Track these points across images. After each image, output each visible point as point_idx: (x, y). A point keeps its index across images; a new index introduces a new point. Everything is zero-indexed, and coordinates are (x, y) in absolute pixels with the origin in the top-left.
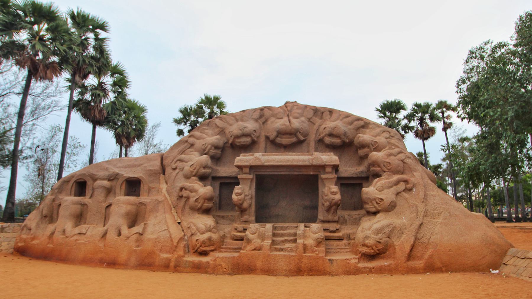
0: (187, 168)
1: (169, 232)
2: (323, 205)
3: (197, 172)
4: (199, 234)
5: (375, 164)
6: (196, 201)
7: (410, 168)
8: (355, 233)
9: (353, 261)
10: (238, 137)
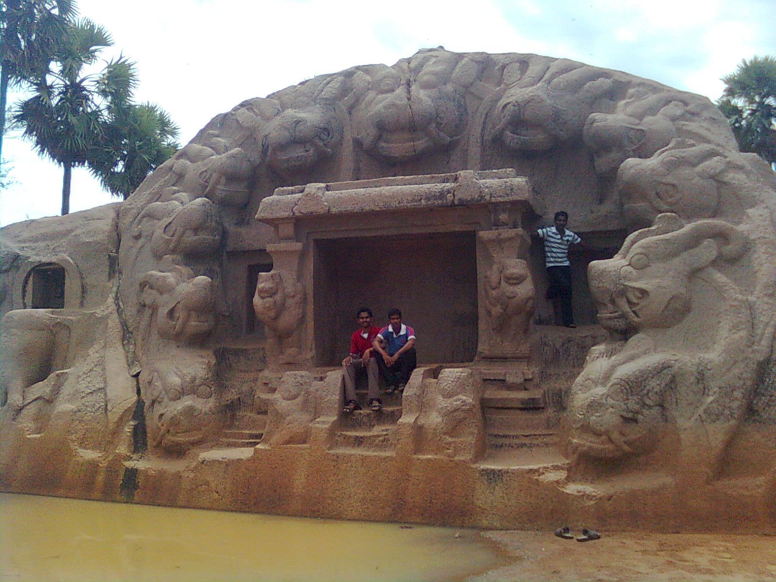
1: (106, 395)
2: (489, 313)
3: (179, 241)
5: (633, 190)
6: (171, 312)
7: (738, 197)
8: (568, 392)
9: (552, 476)
10: (282, 147)
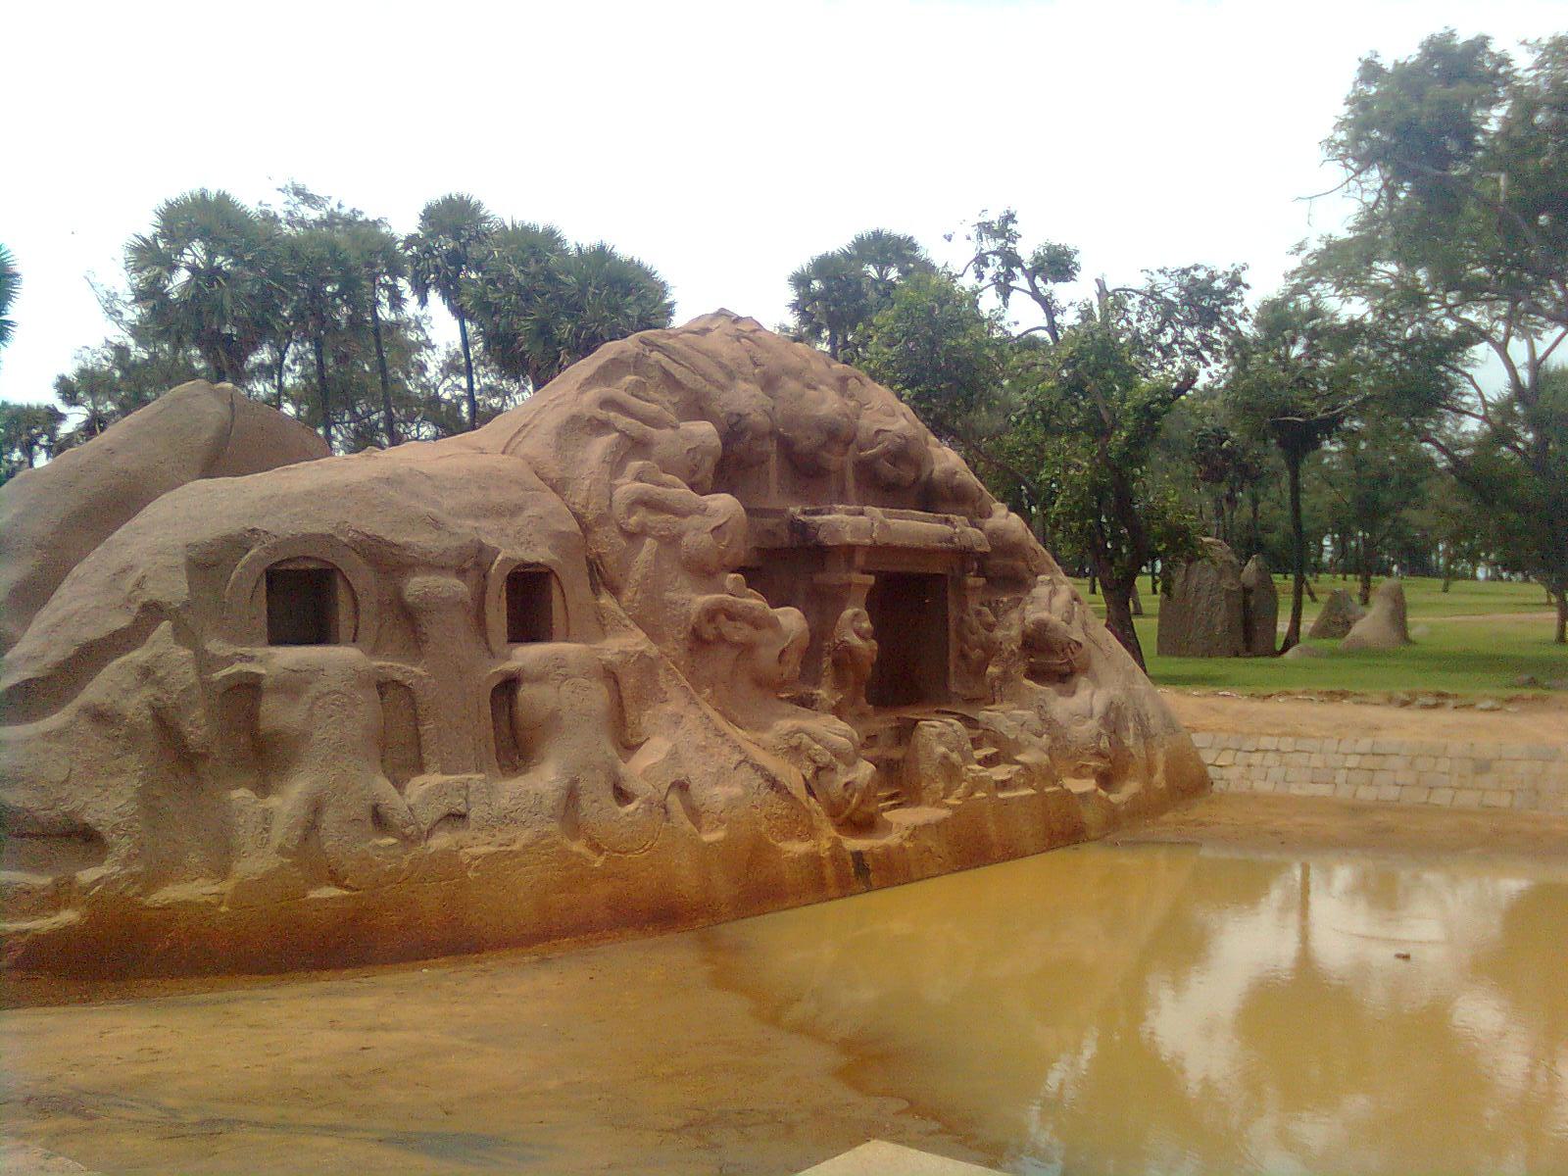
0: (696, 536)
2: (963, 656)
4: (841, 767)
